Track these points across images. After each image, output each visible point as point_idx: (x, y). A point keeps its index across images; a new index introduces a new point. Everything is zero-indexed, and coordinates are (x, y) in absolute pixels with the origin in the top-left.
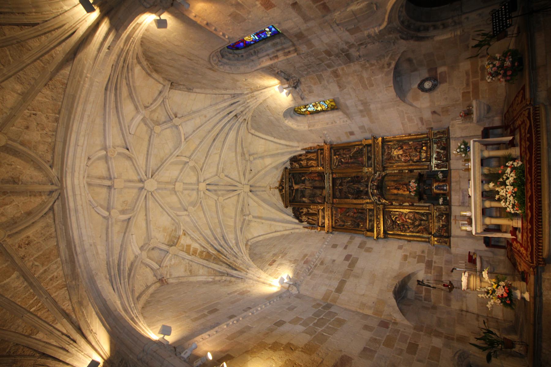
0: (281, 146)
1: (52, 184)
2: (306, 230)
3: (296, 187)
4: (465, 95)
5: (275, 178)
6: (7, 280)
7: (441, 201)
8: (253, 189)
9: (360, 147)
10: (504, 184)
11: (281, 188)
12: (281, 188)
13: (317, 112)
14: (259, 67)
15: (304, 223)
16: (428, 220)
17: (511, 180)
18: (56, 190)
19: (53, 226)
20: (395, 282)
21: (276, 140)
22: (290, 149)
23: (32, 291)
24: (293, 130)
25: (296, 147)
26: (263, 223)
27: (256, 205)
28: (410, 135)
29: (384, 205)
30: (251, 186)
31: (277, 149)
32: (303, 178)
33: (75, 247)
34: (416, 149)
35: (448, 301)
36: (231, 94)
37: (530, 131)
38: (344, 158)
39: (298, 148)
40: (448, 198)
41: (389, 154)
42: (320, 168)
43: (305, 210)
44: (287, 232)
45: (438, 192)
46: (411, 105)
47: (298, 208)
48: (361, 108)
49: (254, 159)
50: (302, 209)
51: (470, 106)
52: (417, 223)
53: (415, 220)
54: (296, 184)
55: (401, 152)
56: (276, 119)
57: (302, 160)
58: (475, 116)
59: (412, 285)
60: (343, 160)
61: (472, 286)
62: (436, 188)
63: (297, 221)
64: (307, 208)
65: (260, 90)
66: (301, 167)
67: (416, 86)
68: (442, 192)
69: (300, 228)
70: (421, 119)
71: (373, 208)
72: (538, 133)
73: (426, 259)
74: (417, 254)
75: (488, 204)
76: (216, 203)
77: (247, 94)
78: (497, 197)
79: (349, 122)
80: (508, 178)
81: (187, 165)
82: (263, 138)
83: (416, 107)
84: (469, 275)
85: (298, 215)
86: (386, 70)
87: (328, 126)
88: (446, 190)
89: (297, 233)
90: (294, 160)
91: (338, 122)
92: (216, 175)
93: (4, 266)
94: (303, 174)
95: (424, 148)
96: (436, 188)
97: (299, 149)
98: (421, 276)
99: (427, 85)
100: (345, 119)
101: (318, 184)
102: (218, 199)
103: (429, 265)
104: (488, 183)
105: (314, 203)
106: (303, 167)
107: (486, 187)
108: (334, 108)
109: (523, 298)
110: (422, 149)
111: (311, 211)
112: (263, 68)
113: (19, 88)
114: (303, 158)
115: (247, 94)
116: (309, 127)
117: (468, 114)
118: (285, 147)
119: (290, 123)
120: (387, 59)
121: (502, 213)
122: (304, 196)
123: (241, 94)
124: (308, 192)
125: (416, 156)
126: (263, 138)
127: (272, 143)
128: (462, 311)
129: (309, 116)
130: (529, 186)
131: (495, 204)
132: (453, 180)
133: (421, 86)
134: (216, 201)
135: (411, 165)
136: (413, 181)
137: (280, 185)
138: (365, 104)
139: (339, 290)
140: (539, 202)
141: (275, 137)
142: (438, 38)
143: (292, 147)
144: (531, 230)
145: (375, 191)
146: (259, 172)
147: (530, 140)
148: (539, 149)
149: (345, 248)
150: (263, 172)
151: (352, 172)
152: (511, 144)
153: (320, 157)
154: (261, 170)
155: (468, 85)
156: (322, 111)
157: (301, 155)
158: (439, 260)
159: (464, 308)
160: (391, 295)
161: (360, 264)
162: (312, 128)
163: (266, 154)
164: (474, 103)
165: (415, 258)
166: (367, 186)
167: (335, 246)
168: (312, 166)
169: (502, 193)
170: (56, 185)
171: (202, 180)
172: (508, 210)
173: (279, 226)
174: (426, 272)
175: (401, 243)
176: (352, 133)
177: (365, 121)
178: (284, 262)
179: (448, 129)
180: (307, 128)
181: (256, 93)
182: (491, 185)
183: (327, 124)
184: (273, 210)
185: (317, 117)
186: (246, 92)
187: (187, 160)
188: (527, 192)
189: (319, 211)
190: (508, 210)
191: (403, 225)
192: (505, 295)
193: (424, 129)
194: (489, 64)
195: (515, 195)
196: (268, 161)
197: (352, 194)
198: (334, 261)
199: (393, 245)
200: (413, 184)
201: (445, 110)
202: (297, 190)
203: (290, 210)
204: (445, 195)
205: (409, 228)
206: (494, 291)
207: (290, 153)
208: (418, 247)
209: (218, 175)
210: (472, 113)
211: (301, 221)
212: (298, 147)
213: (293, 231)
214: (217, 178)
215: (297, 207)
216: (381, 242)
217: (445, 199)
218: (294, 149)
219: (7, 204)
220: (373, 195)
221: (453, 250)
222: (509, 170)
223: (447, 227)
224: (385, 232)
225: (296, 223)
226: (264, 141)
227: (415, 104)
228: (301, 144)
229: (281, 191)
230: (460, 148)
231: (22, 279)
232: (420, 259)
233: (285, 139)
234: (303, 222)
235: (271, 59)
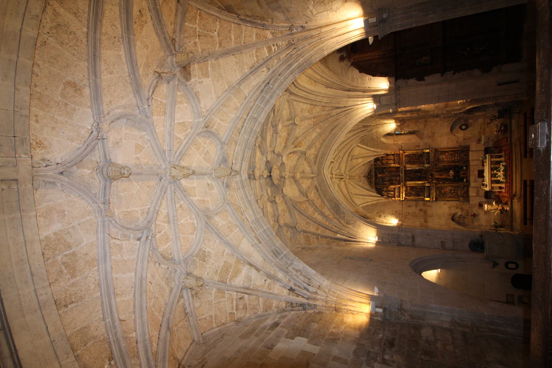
0: (370, 152)
1: (312, 174)
2: (387, 200)
3: (379, 176)
4: (480, 133)
5: (366, 169)
6: (315, 216)
7: (465, 180)
8: (350, 178)
9: (422, 153)
10: (499, 171)
11: (369, 176)
12: (369, 177)
13: (401, 134)
14: (394, 117)
15: (384, 197)
16: (458, 190)
17: (502, 169)
18: (315, 177)
19: (317, 193)
20: (451, 217)
21: (368, 148)
22: (375, 154)
23: (325, 220)
24: (384, 143)
25: (379, 152)
26: (358, 198)
27: (352, 187)
28: (449, 148)
29: (435, 183)
30: (349, 176)
31: (367, 153)
32: (385, 170)
33: (337, 201)
34: (452, 155)
35: (473, 222)
36: (363, 125)
37: (509, 153)
38: (411, 159)
39: (381, 152)
40: (468, 179)
41: (438, 157)
42: (397, 165)
43: (385, 189)
44: (375, 202)
45: (464, 176)
46: (455, 135)
47: (380, 188)
48: (430, 135)
49: (354, 159)
50: (383, 188)
51: (481, 137)
52: (453, 192)
53: (452, 190)
54: (379, 174)
55: (444, 156)
56: (377, 137)
57: (384, 160)
58: (482, 142)
59: (456, 218)
60: (411, 160)
61: (489, 208)
62: (463, 174)
63: (380, 196)
64: (387, 188)
65: (382, 124)
66: (382, 164)
67: (458, 127)
68: (465, 176)
69: (383, 200)
70: (457, 142)
71: (429, 185)
72: (512, 154)
73: (460, 207)
74: (454, 206)
75: (493, 179)
76: (339, 186)
77: (374, 126)
78: (497, 176)
79: (420, 141)
80: (501, 169)
81: (332, 163)
82: (359, 147)
83: (457, 136)
84: (488, 205)
85: (380, 192)
86: (450, 121)
87: (406, 142)
88: (467, 175)
89: (382, 202)
90: (376, 160)
91: (413, 140)
92: (338, 169)
93: (312, 209)
94: (385, 168)
95: (456, 155)
96: (463, 174)
97: (382, 153)
98: (459, 213)
99: (463, 127)
100: (417, 139)
101: (393, 173)
102: (340, 183)
103: (462, 209)
104: (494, 171)
105: (393, 184)
106: (383, 164)
107: (492, 172)
108: (410, 133)
109: (507, 210)
110: (455, 155)
111: (389, 190)
112: (396, 118)
113: (318, 130)
114: (384, 159)
115: (374, 126)
116: (394, 142)
117: (479, 141)
118: (372, 152)
119: (383, 140)
120: (452, 118)
121: (498, 182)
122: (384, 181)
123: (370, 126)
124: (387, 179)
125: (452, 159)
126: (359, 147)
127: (365, 150)
128: (479, 225)
129: (395, 136)
130: (509, 171)
131: (495, 179)
132: (471, 170)
133: (461, 128)
134: (338, 184)
135: (450, 163)
136: (452, 171)
137: (368, 175)
138: (433, 133)
139: (426, 221)
140: (512, 177)
141: (367, 146)
142: (476, 114)
143: (377, 152)
144: (510, 186)
145: (430, 177)
146: (354, 167)
147: (509, 156)
148: (512, 159)
149: (416, 206)
150: (357, 167)
151: (415, 167)
152: (500, 157)
153: (396, 158)
154: (356, 165)
155: (481, 128)
156: (404, 134)
157: (382, 157)
158: (466, 206)
159: (480, 224)
160: (451, 221)
161: (429, 212)
162: (396, 143)
163: (360, 156)
164: (483, 137)
165: (454, 207)
166: (426, 174)
167: (410, 206)
168: (392, 164)
169: (499, 174)
170: (315, 174)
171: (333, 172)
172: (501, 180)
173: (369, 199)
174: (461, 212)
175: (445, 202)
176: (418, 146)
177: (429, 141)
178: (387, 215)
179: (469, 146)
180: (392, 142)
181: (379, 126)
182: (495, 171)
183: (406, 141)
184: (364, 190)
185: (400, 137)
186: (373, 125)
187: (333, 160)
188: (508, 173)
189: (395, 188)
190: (501, 180)
191: (445, 193)
192: (501, 209)
193: (457, 145)
194: (496, 128)
195: (504, 175)
196: (360, 160)
197: (416, 178)
198: (414, 212)
199: (441, 203)
200: (451, 172)
201: (470, 138)
202: (379, 177)
203: (374, 190)
204: (466, 178)
205: (448, 194)
206: (497, 208)
207: (375, 156)
208: (454, 203)
209: (340, 169)
210: (482, 141)
211: (382, 195)
212: (381, 152)
213: (378, 201)
214: (338, 171)
215: (379, 187)
216: (433, 202)
217: (467, 179)
218: (379, 153)
219: (303, 183)
220: (429, 178)
221: (471, 202)
222: (501, 166)
223: (467, 192)
224: (435, 197)
225: (378, 197)
226: (360, 148)
227: (456, 135)
228: (383, 150)
229: (369, 178)
230: (482, 157)
231: (319, 216)
232: (457, 208)
233: (373, 147)
234: (384, 196)
235: (402, 115)
